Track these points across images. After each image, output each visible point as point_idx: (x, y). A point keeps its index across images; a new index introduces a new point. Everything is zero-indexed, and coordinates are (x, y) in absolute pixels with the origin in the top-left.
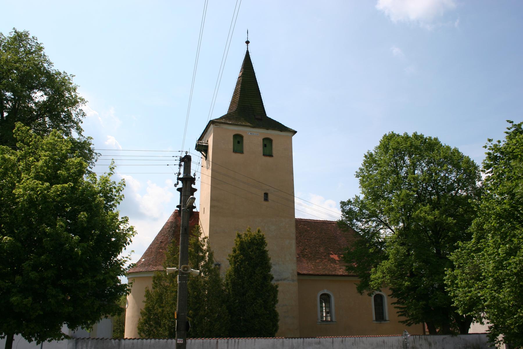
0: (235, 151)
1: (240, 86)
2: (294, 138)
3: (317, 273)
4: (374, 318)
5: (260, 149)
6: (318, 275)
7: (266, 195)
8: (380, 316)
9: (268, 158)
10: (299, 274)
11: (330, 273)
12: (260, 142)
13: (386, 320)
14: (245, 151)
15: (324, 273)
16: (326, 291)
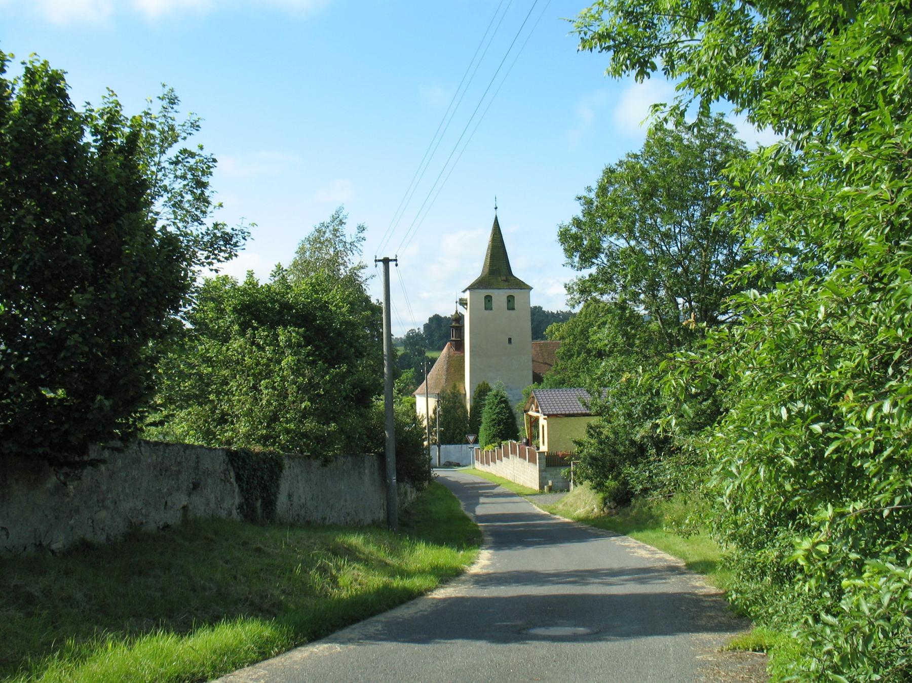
0: (486, 309)
2: (532, 292)
5: (505, 305)
9: (511, 311)
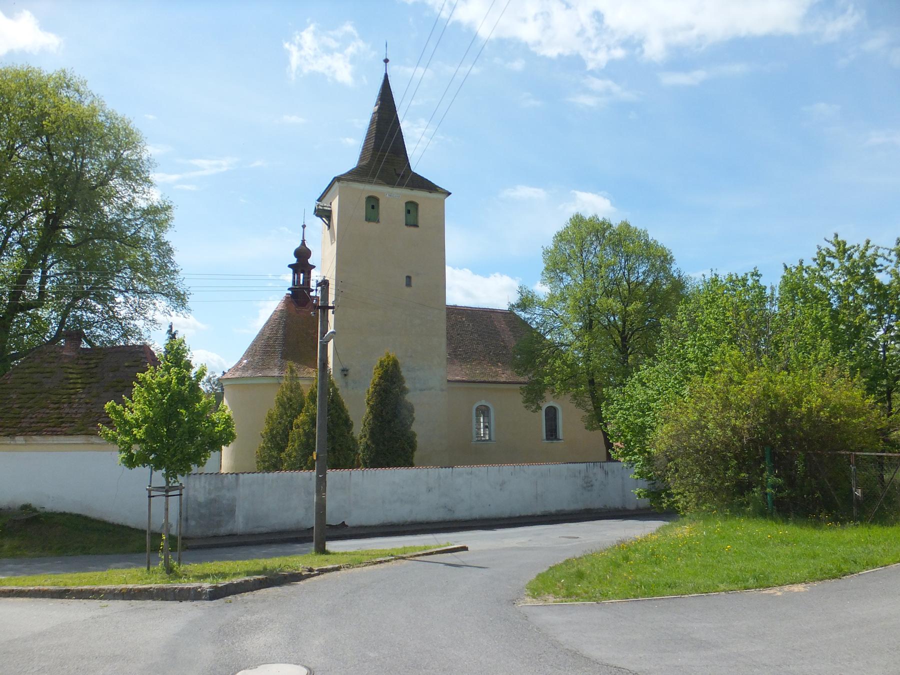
0: (368, 219)
1: (375, 127)
2: (448, 201)
3: (473, 379)
4: (545, 437)
6: (474, 382)
7: (409, 278)
8: (552, 433)
10: (449, 381)
11: (490, 380)
13: (559, 440)
14: (380, 220)
15: (482, 380)
16: (483, 403)
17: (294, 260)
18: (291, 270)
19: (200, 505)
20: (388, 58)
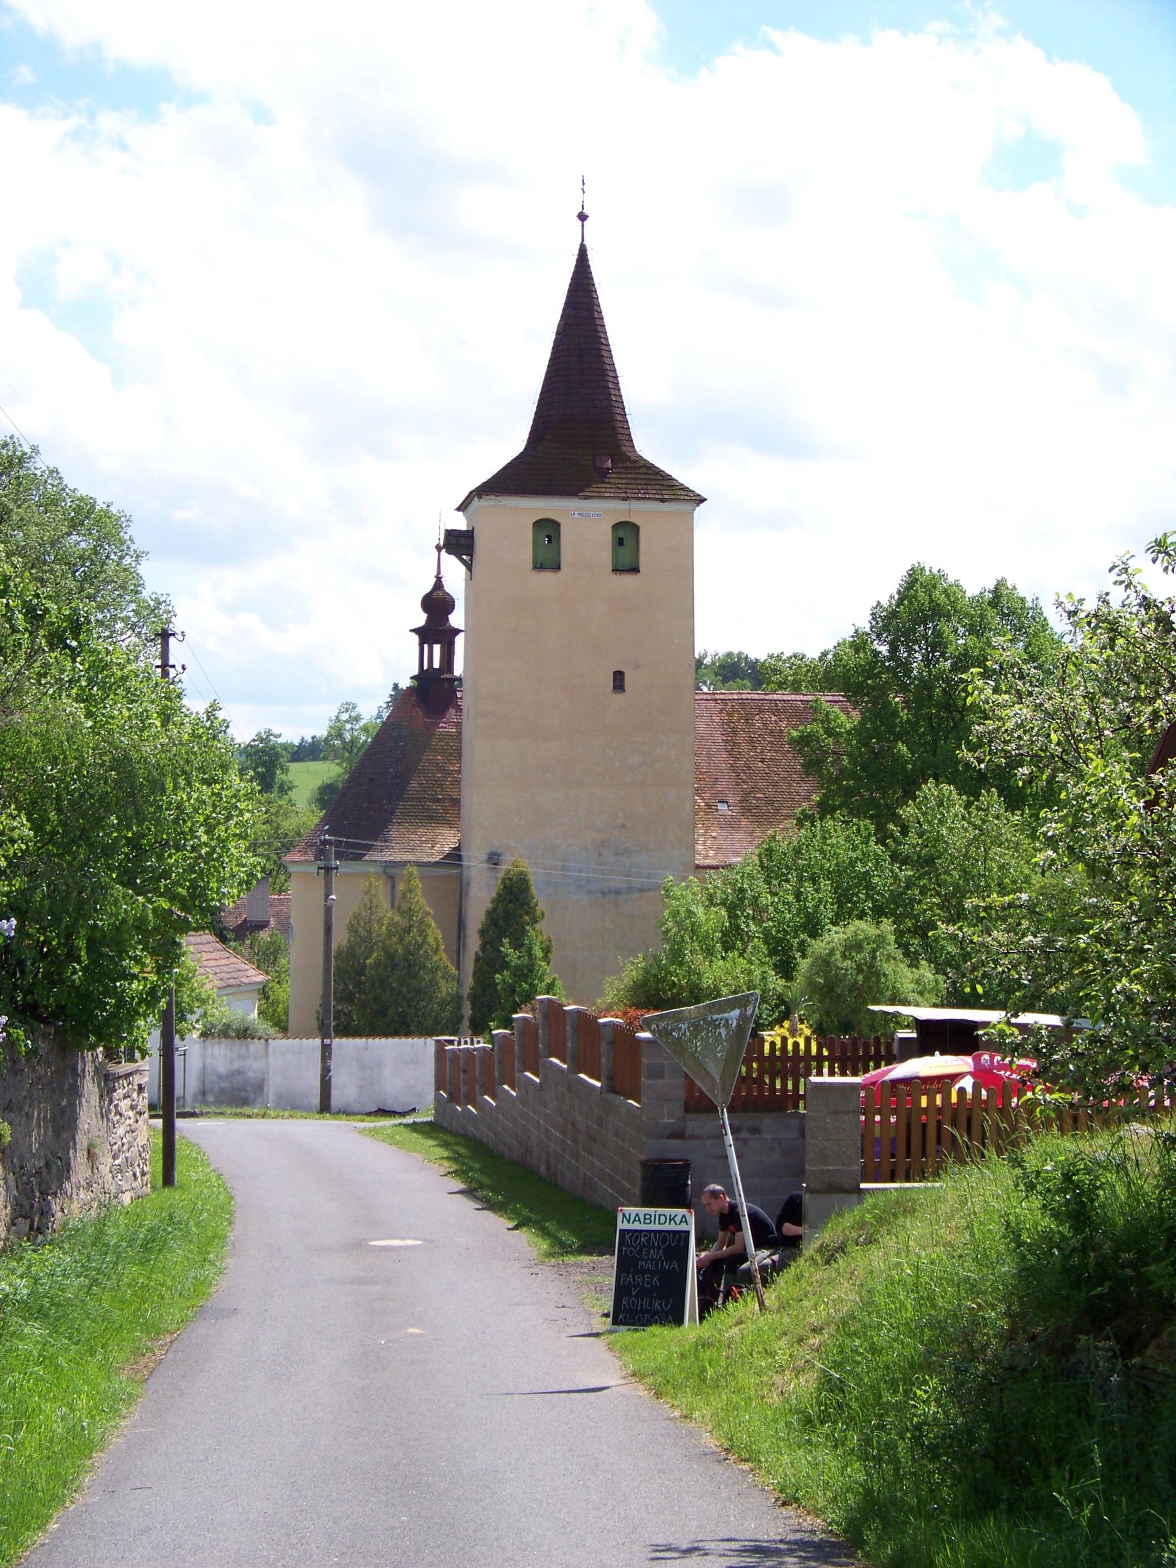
0: (539, 566)
2: (700, 511)
9: (628, 579)
12: (606, 537)
17: (421, 619)
18: (415, 638)
19: (220, 1077)
20: (585, 211)
